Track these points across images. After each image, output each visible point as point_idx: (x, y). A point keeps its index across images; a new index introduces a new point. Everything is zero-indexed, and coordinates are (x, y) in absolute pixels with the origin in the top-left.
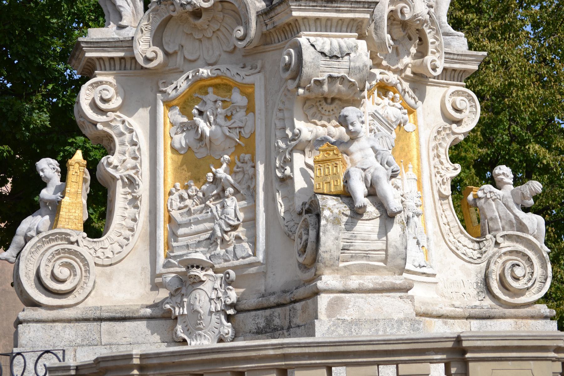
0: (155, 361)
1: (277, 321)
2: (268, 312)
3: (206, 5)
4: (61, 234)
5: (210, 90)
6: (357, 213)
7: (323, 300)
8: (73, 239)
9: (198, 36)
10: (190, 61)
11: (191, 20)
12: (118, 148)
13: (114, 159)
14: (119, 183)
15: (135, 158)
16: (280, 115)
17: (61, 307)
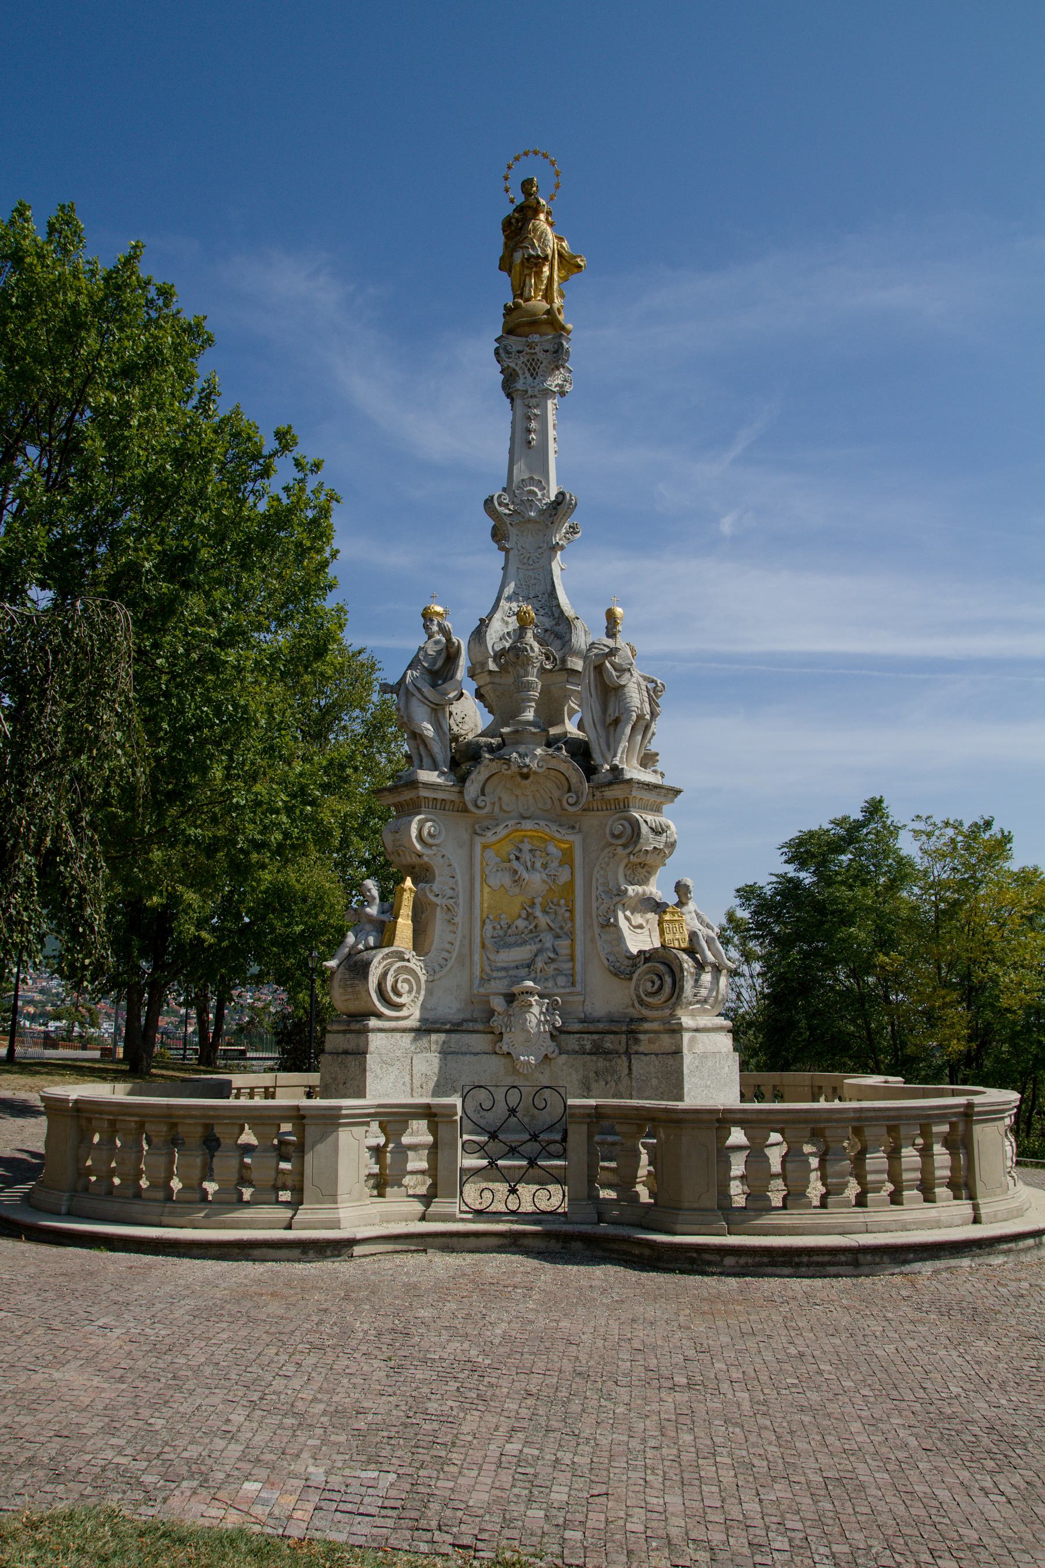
0: (739, 1116)
1: (608, 1045)
2: (596, 1037)
3: (540, 770)
4: (397, 952)
5: (526, 840)
6: (700, 966)
7: (686, 1036)
8: (406, 957)
9: (518, 792)
10: (506, 812)
11: (519, 779)
12: (437, 879)
13: (436, 887)
14: (439, 909)
15: (453, 889)
16: (602, 872)
17: (397, 1019)
